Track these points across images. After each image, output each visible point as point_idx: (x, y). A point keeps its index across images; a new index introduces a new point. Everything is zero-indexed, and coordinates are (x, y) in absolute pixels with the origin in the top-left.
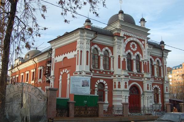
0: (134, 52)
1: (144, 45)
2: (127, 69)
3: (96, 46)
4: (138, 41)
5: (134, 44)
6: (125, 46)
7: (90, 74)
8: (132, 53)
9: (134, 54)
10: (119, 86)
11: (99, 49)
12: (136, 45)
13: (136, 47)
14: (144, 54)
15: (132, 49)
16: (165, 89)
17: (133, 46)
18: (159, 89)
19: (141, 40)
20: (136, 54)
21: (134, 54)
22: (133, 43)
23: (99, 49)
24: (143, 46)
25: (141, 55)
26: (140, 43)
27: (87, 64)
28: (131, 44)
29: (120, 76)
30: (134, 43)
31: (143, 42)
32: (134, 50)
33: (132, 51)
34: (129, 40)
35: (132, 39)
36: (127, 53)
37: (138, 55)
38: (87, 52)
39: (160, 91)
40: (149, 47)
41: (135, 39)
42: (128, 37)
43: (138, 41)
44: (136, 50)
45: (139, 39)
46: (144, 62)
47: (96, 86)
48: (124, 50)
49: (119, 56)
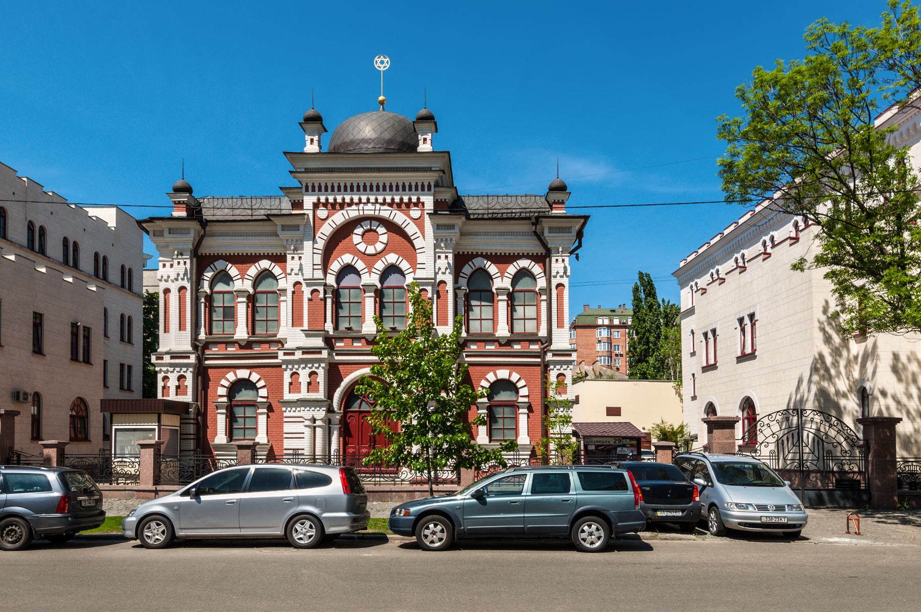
1: (419, 222)
2: (329, 326)
6: (321, 244)
7: (188, 357)
8: (360, 265)
9: (370, 267)
10: (294, 386)
12: (381, 230)
13: (384, 238)
14: (420, 258)
15: (362, 247)
18: (522, 383)
20: (380, 266)
21: (370, 267)
24: (411, 229)
25: (404, 265)
26: (399, 218)
27: (181, 327)
28: (359, 231)
29: (293, 354)
30: (375, 223)
31: (415, 213)
32: (371, 250)
33: (364, 255)
34: (339, 218)
35: (353, 213)
36: (335, 266)
37: (392, 269)
38: (182, 289)
39: (219, 388)
41: (369, 210)
42: (334, 207)
43: (385, 212)
44: (379, 247)
47: (222, 391)
48: (318, 259)
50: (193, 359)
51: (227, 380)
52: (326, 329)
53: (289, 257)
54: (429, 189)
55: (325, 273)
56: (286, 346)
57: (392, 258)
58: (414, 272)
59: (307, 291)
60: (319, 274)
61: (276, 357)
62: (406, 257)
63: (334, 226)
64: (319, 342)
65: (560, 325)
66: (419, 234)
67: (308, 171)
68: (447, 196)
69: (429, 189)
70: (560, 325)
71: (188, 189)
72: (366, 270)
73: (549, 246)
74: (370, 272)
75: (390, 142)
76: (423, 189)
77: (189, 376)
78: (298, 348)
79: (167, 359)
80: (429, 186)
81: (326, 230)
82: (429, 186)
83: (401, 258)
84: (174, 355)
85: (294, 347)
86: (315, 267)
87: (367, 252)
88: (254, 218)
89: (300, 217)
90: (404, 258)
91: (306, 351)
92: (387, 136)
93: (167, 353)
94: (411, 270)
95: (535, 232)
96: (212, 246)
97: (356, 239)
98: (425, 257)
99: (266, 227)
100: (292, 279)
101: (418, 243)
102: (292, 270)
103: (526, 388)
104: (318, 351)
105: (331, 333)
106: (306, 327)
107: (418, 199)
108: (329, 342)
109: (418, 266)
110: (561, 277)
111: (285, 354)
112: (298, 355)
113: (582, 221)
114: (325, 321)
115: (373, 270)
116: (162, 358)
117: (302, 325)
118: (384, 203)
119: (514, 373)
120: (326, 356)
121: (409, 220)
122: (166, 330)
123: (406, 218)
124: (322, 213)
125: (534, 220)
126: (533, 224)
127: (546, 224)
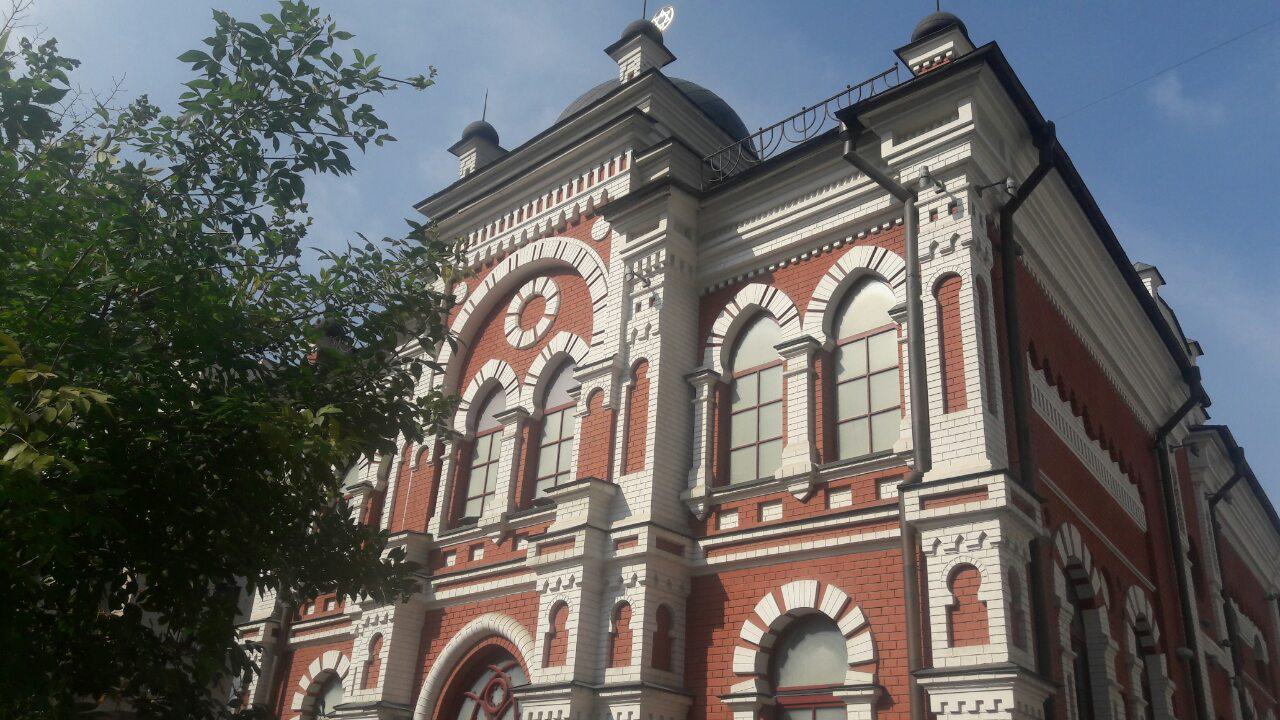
0: (521, 358)
5: (538, 289)
8: (507, 377)
9: (521, 374)
14: (599, 321)
16: (939, 597)
18: (854, 618)
20: (538, 366)
22: (526, 290)
28: (515, 305)
34: (480, 293)
35: (501, 271)
41: (525, 256)
43: (549, 248)
44: (543, 325)
57: (558, 343)
65: (953, 401)
70: (953, 401)
83: (574, 337)
98: (607, 320)
101: (596, 292)
103: (866, 636)
110: (945, 252)
114: (431, 513)
118: (550, 234)
119: (830, 588)
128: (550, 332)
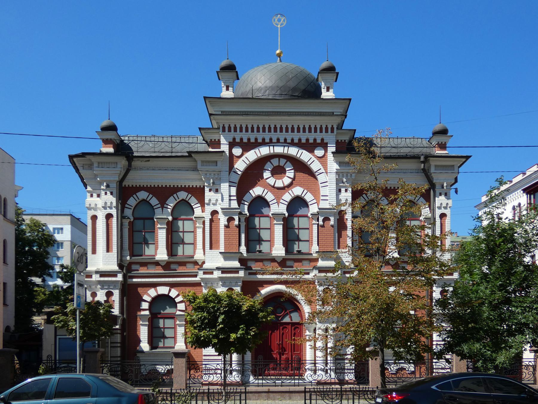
1: (322, 159)
2: (243, 249)
3: (143, 195)
4: (293, 151)
5: (282, 164)
7: (116, 276)
8: (269, 197)
11: (154, 201)
14: (323, 191)
15: (271, 181)
17: (278, 171)
19: (310, 147)
20: (287, 197)
22: (275, 162)
23: (154, 201)
24: (315, 166)
25: (309, 197)
26: (305, 156)
28: (269, 166)
29: (212, 273)
30: (283, 161)
31: (319, 152)
32: (279, 184)
34: (252, 156)
35: (265, 151)
40: (340, 164)
41: (279, 150)
43: (293, 151)
44: (287, 181)
45: (300, 145)
46: (318, 221)
49: (214, 213)
50: (120, 278)
51: (149, 296)
52: (241, 251)
53: (207, 190)
54: (332, 131)
55: (239, 203)
56: (205, 266)
57: (297, 191)
58: (318, 203)
59: (223, 220)
60: (234, 204)
61: (196, 276)
62: (310, 190)
63: (248, 163)
64: (236, 264)
66: (323, 170)
67: (224, 114)
68: (346, 138)
69: (332, 131)
71: (112, 128)
72: (275, 201)
73: (434, 181)
74: (278, 203)
75: (294, 89)
76: (327, 131)
77: (116, 294)
78: (218, 269)
79: (96, 278)
80: (332, 128)
81: (240, 166)
82: (332, 128)
83: (305, 191)
84: (103, 274)
85: (215, 267)
86: (232, 198)
87: (276, 186)
88: (174, 154)
89: (220, 154)
90: (308, 191)
91: (224, 270)
92: (292, 84)
93: (97, 272)
94: (315, 201)
95: (424, 170)
96: (136, 178)
97: (267, 174)
99: (187, 163)
100: (209, 209)
101: (321, 178)
102: (210, 200)
104: (235, 270)
105: (245, 255)
106: (222, 250)
107: (322, 140)
108: (243, 261)
109: (322, 198)
111: (205, 273)
112: (217, 274)
113: (464, 160)
114: (240, 245)
115: (282, 201)
116: (91, 277)
117: (218, 248)
120: (243, 275)
121: (313, 158)
122: (94, 252)
123: (312, 156)
124: (237, 151)
125: (422, 159)
126: (422, 162)
127: (433, 162)
128: (290, 186)
